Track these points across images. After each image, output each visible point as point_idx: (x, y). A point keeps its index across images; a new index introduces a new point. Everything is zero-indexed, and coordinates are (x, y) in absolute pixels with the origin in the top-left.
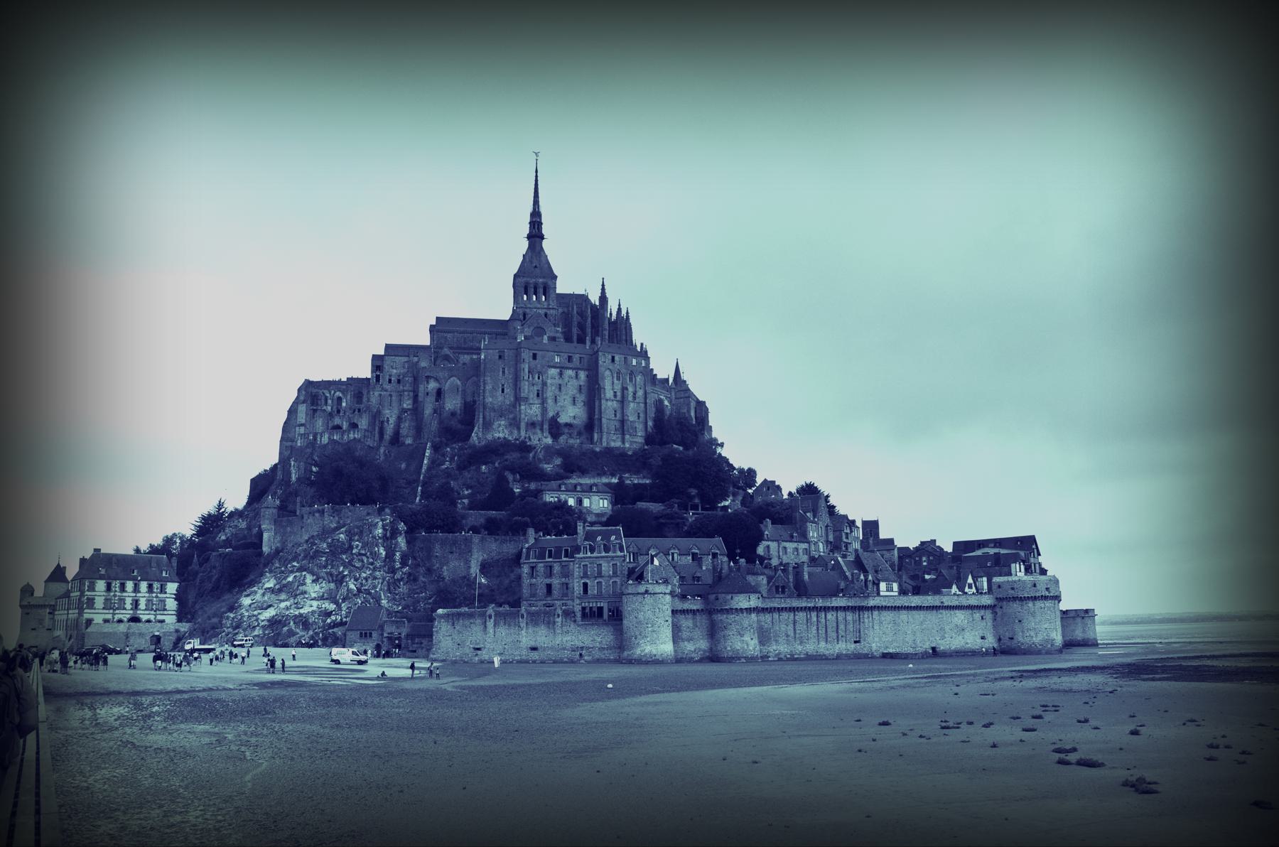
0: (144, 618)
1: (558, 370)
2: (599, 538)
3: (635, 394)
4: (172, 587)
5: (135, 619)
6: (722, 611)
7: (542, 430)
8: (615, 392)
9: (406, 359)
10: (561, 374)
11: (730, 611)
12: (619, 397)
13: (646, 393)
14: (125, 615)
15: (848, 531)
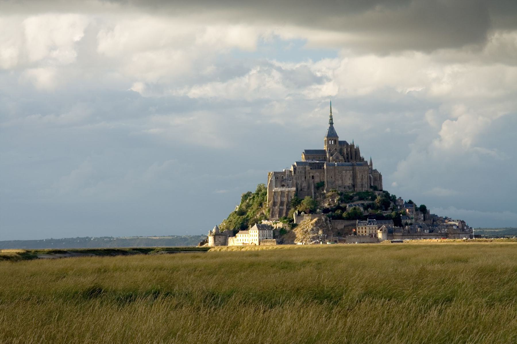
0: (268, 238)
1: (345, 171)
2: (371, 222)
3: (365, 176)
4: (272, 231)
5: (267, 239)
6: (395, 236)
7: (342, 187)
8: (360, 177)
9: (302, 166)
10: (346, 172)
11: (397, 236)
12: (361, 178)
13: (368, 177)
14: (265, 237)
15: (420, 215)
